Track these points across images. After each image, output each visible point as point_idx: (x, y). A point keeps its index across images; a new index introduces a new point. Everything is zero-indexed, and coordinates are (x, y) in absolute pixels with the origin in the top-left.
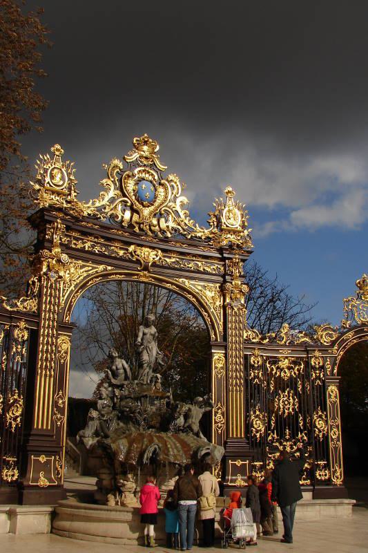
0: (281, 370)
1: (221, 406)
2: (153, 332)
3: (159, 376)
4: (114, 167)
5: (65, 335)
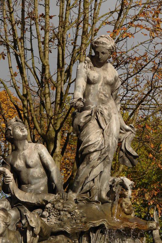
2: (110, 78)
3: (128, 182)
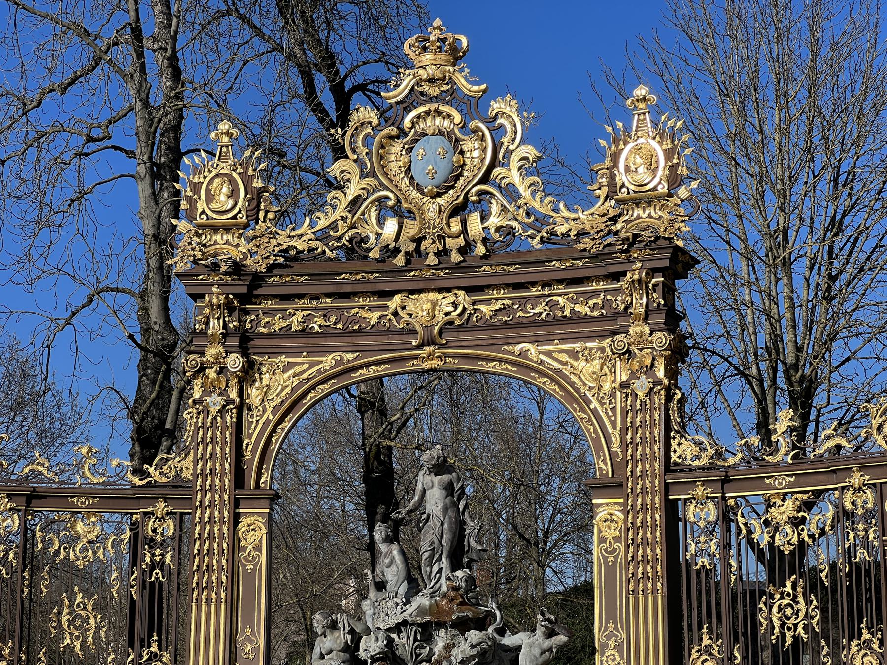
0: (776, 529)
1: (616, 628)
4: (356, 129)
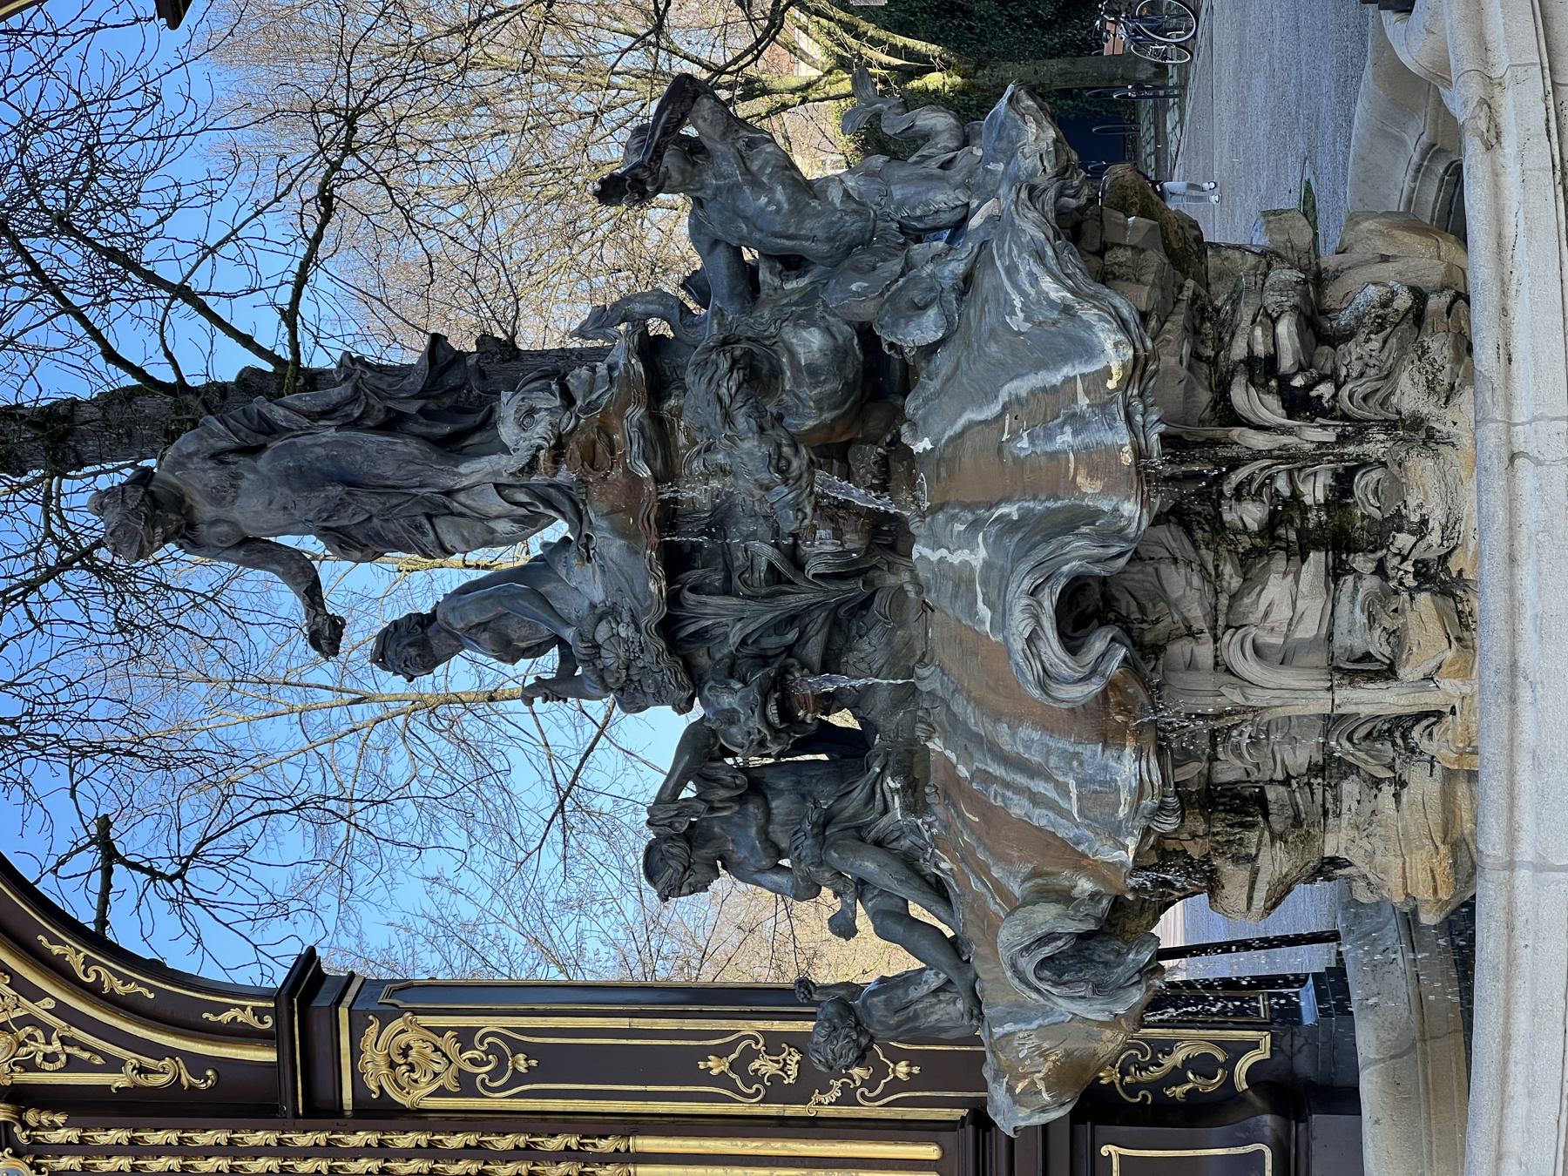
5: (356, 1053)
